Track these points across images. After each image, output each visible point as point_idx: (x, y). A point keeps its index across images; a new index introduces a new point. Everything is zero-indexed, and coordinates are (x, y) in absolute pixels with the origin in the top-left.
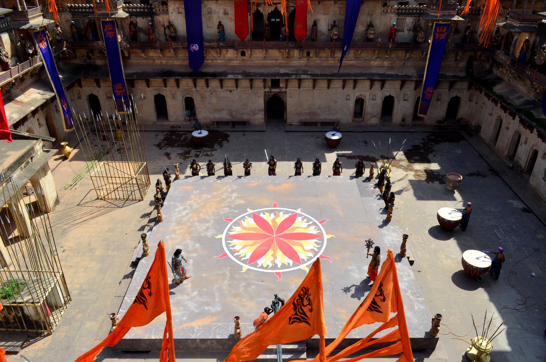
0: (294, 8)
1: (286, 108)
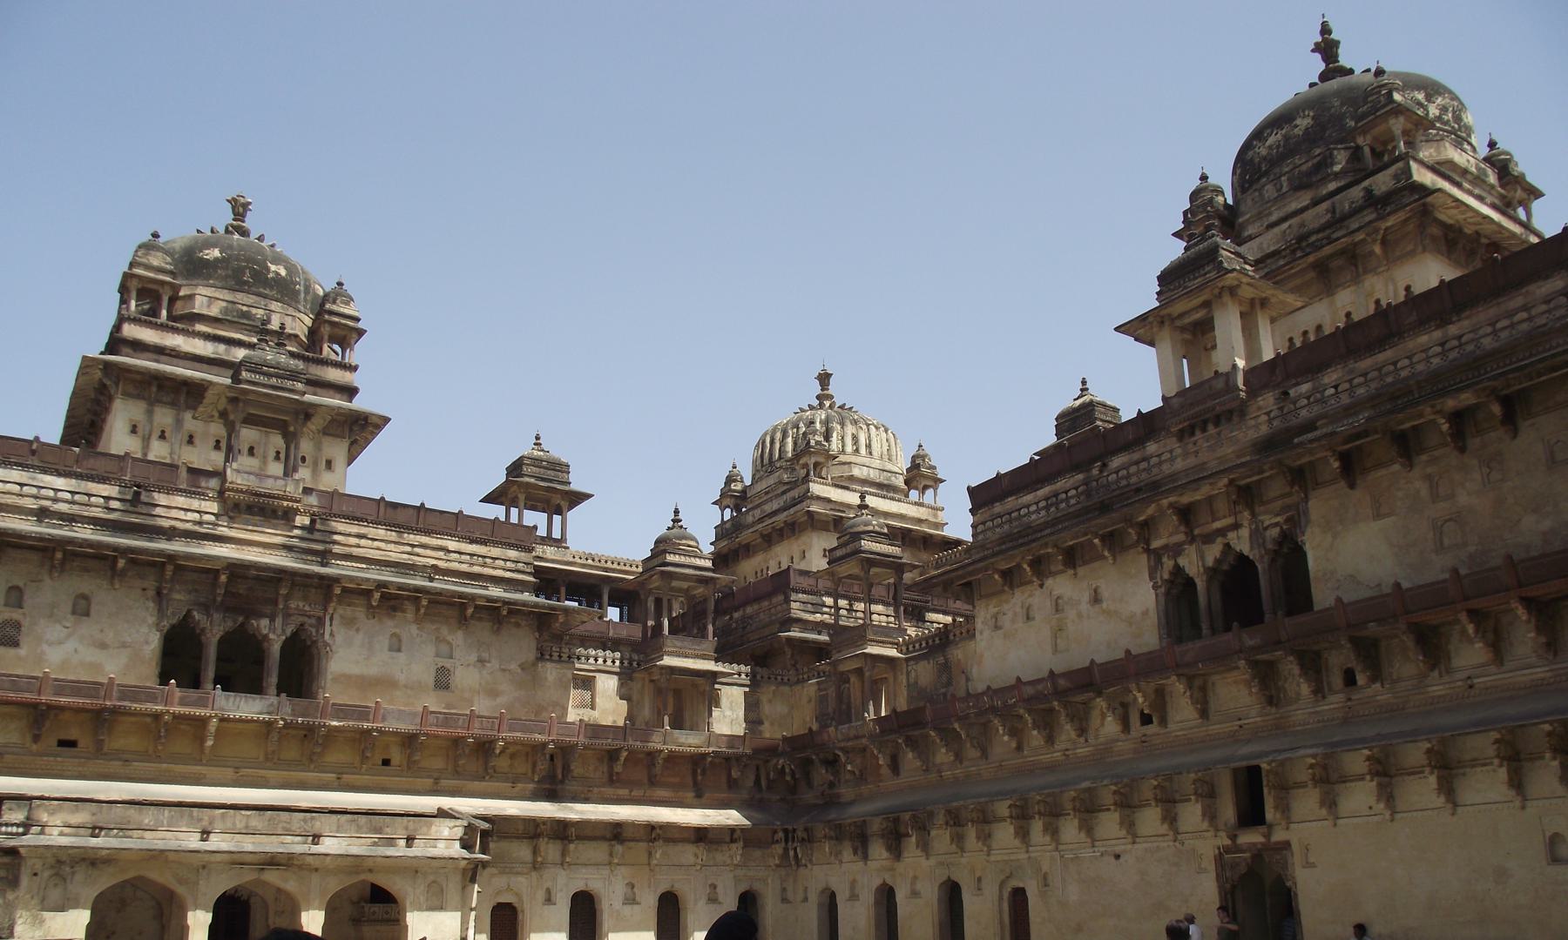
0: (1277, 530)
1: (1299, 912)
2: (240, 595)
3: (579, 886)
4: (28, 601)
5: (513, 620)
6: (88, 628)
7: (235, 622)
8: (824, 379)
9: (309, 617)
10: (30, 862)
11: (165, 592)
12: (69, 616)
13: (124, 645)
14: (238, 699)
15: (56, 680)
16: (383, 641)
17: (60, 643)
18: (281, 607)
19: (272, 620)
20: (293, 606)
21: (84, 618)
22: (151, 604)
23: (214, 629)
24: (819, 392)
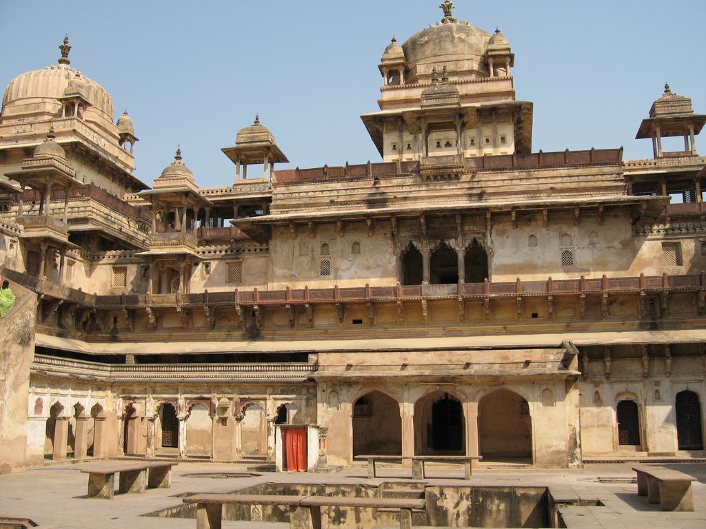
2: (437, 228)
3: (681, 388)
4: (331, 250)
5: (612, 214)
6: (360, 260)
7: (436, 243)
9: (478, 233)
10: (320, 385)
11: (395, 233)
12: (350, 255)
13: (378, 266)
14: (435, 288)
15: (341, 289)
16: (526, 240)
18: (459, 230)
19: (456, 239)
20: (466, 229)
22: (390, 242)
23: (425, 249)
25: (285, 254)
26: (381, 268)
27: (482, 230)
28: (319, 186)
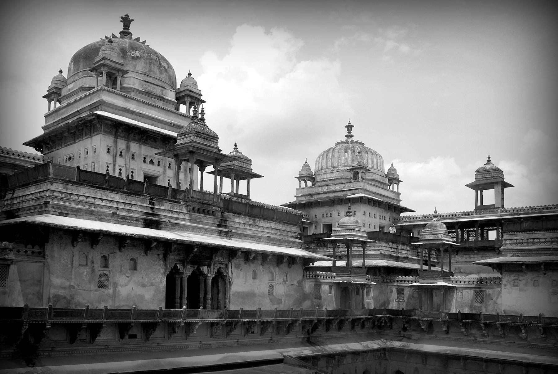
4: (111, 264)
6: (137, 277)
8: (349, 127)
9: (222, 264)
12: (128, 271)
13: (152, 285)
16: (251, 274)
17: (126, 286)
19: (209, 266)
21: (135, 271)
22: (162, 263)
24: (347, 134)
25: (63, 262)
26: (154, 287)
27: (226, 261)
28: (99, 194)
